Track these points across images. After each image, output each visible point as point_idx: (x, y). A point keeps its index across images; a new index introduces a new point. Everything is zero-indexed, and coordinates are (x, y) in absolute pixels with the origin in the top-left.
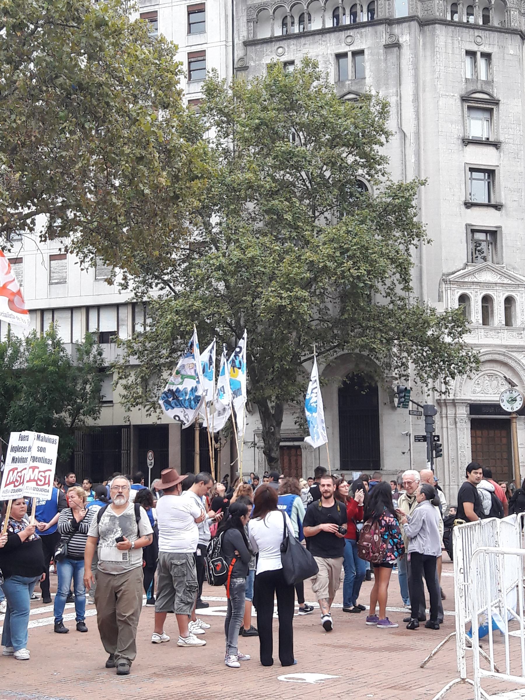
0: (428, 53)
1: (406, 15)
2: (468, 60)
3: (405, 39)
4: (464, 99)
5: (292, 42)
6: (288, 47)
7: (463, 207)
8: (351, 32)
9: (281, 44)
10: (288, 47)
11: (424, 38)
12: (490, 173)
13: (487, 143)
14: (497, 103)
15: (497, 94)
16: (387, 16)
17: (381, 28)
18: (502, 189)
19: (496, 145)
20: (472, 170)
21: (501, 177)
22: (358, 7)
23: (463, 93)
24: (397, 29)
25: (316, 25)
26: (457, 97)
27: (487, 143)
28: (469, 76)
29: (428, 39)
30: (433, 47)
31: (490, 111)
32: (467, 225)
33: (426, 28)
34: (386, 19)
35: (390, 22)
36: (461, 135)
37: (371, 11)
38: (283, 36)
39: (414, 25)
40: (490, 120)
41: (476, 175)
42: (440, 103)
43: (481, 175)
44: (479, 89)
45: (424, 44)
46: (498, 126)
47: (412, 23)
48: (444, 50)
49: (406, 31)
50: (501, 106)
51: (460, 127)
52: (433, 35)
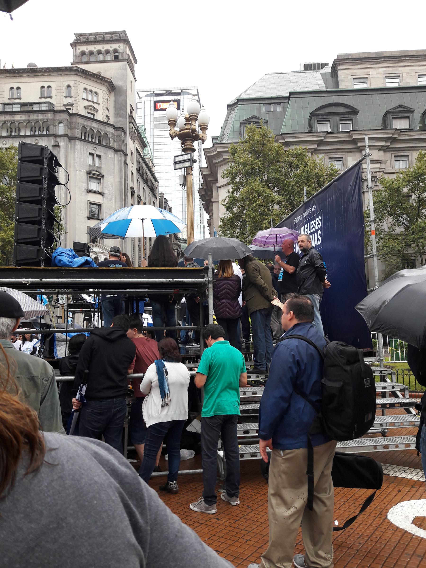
0: (72, 152)
1: (63, 134)
2: (91, 157)
3: (62, 144)
4: (88, 173)
5: (10, 139)
6: (8, 141)
7: (86, 219)
8: (38, 138)
9: (5, 139)
10: (8, 141)
11: (71, 144)
12: (100, 206)
13: (98, 193)
14: (103, 176)
15: (103, 173)
16: (54, 133)
17: (51, 138)
18: (104, 213)
19: (102, 194)
20: (91, 203)
21: (104, 207)
22: (41, 128)
23: (88, 170)
24: (58, 139)
25: (22, 133)
26: (85, 171)
27: (98, 193)
28: (91, 163)
29: (73, 146)
30: (75, 148)
31: (100, 179)
32: (88, 227)
33: (72, 141)
34: (54, 134)
35: (55, 136)
36: (86, 188)
37: (47, 130)
38: (7, 136)
39: (66, 139)
40: (100, 183)
41: (93, 206)
42: (77, 173)
43: (95, 206)
44: (95, 169)
45: (71, 148)
46: (103, 186)
47: (65, 138)
48: (79, 151)
49: (62, 140)
50: (105, 178)
51: (86, 184)
52: (75, 144)
